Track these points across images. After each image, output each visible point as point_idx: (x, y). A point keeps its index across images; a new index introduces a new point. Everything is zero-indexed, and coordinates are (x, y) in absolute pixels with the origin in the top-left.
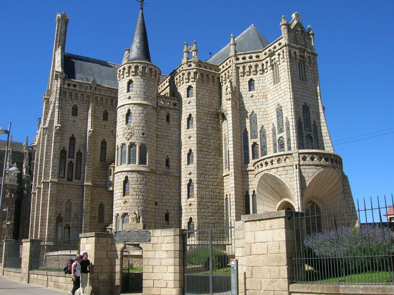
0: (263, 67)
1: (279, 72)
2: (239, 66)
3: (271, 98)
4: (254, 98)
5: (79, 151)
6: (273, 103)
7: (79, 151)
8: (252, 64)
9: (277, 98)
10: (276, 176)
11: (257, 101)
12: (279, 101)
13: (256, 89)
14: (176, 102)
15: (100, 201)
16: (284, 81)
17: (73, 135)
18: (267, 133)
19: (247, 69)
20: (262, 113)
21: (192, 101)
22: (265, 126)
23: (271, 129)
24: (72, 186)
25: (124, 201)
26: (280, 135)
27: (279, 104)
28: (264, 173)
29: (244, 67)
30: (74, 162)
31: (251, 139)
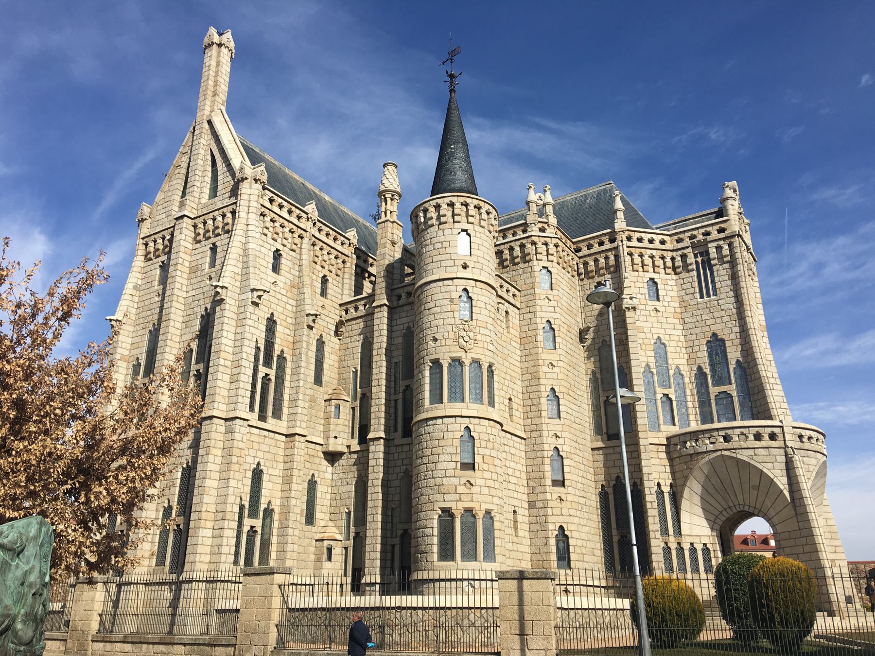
0: (673, 264)
1: (716, 279)
2: (633, 250)
3: (694, 319)
4: (660, 314)
5: (282, 351)
6: (699, 330)
7: (282, 351)
8: (654, 252)
9: (708, 323)
10: (752, 462)
11: (664, 320)
12: (713, 328)
13: (661, 298)
14: (517, 293)
15: (311, 472)
16: (729, 295)
17: (272, 314)
18: (687, 380)
19: (648, 261)
20: (674, 344)
21: (551, 297)
22: (682, 368)
23: (693, 373)
24: (266, 433)
25: (463, 480)
26: (722, 389)
27: (714, 335)
28: (719, 453)
29: (641, 255)
30: (273, 378)
31: (659, 387)
